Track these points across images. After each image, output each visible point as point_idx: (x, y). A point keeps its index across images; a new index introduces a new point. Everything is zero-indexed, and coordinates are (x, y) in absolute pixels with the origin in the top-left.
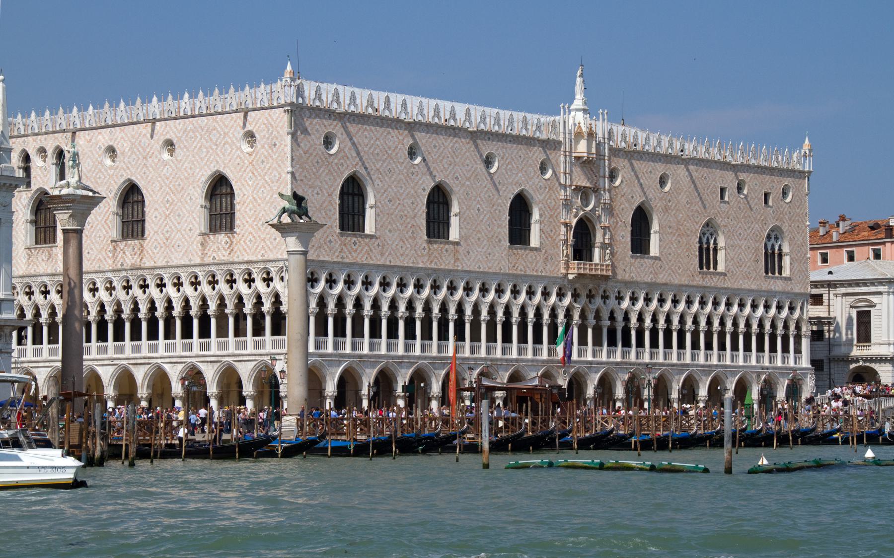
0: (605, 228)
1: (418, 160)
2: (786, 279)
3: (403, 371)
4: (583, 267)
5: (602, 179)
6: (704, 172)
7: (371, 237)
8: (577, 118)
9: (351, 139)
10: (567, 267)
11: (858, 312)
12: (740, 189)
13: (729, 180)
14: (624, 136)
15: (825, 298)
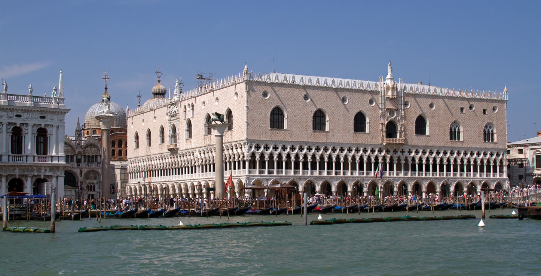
0: (402, 125)
1: (374, 104)
2: (495, 143)
3: (302, 182)
4: (391, 140)
5: (400, 106)
6: (453, 101)
7: (286, 130)
8: (389, 82)
9: (276, 93)
10: (383, 140)
11: (536, 156)
12: (471, 108)
13: (466, 105)
14: (411, 88)
15: (524, 151)
